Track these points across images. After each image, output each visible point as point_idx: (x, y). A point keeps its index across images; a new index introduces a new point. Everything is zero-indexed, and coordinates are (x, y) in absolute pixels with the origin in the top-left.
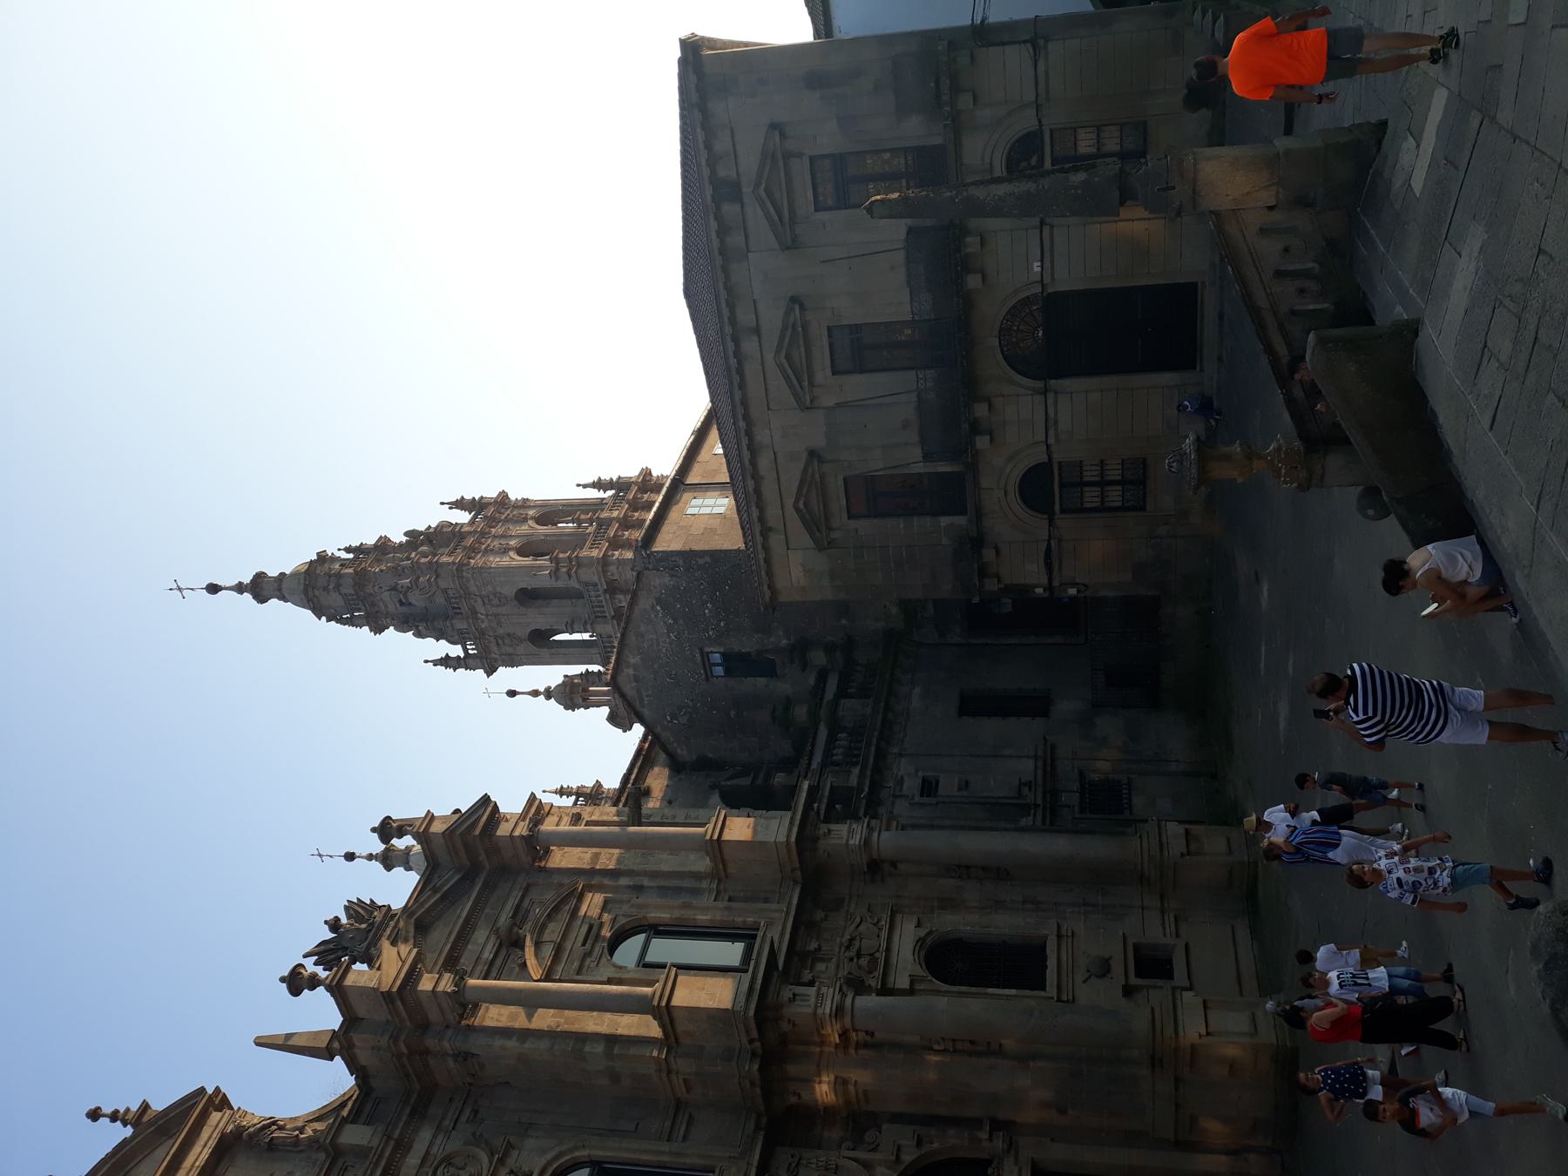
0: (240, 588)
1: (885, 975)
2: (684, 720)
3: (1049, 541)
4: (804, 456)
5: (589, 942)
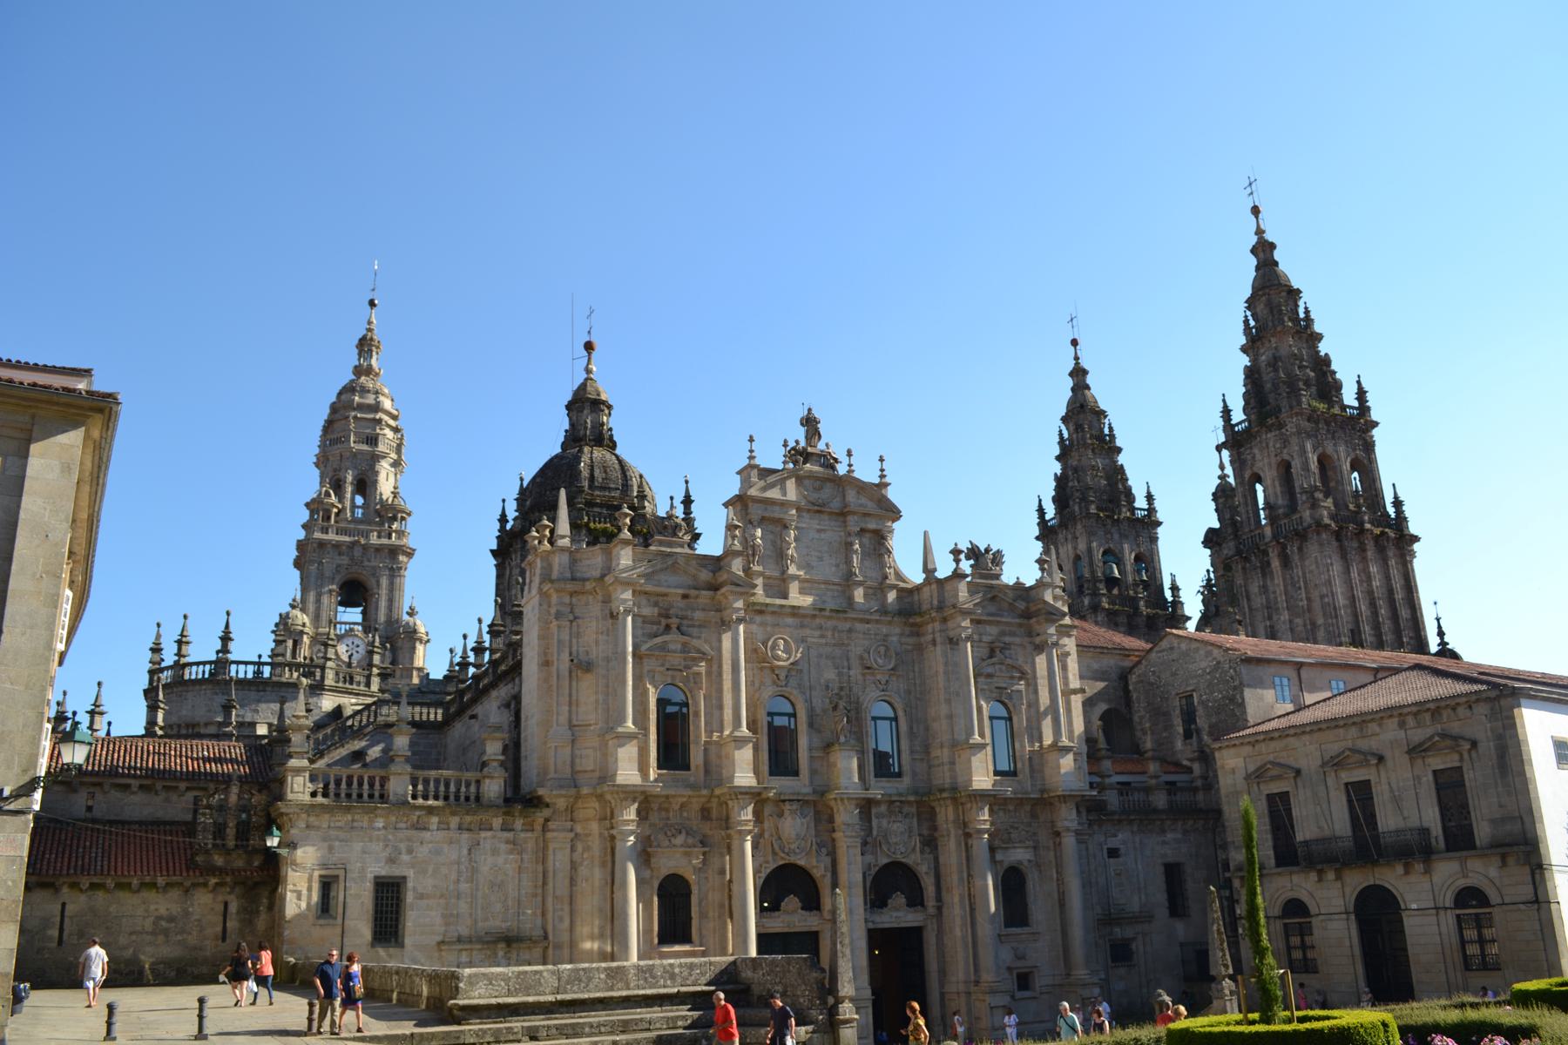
0: (1259, 232)
2: (1152, 679)
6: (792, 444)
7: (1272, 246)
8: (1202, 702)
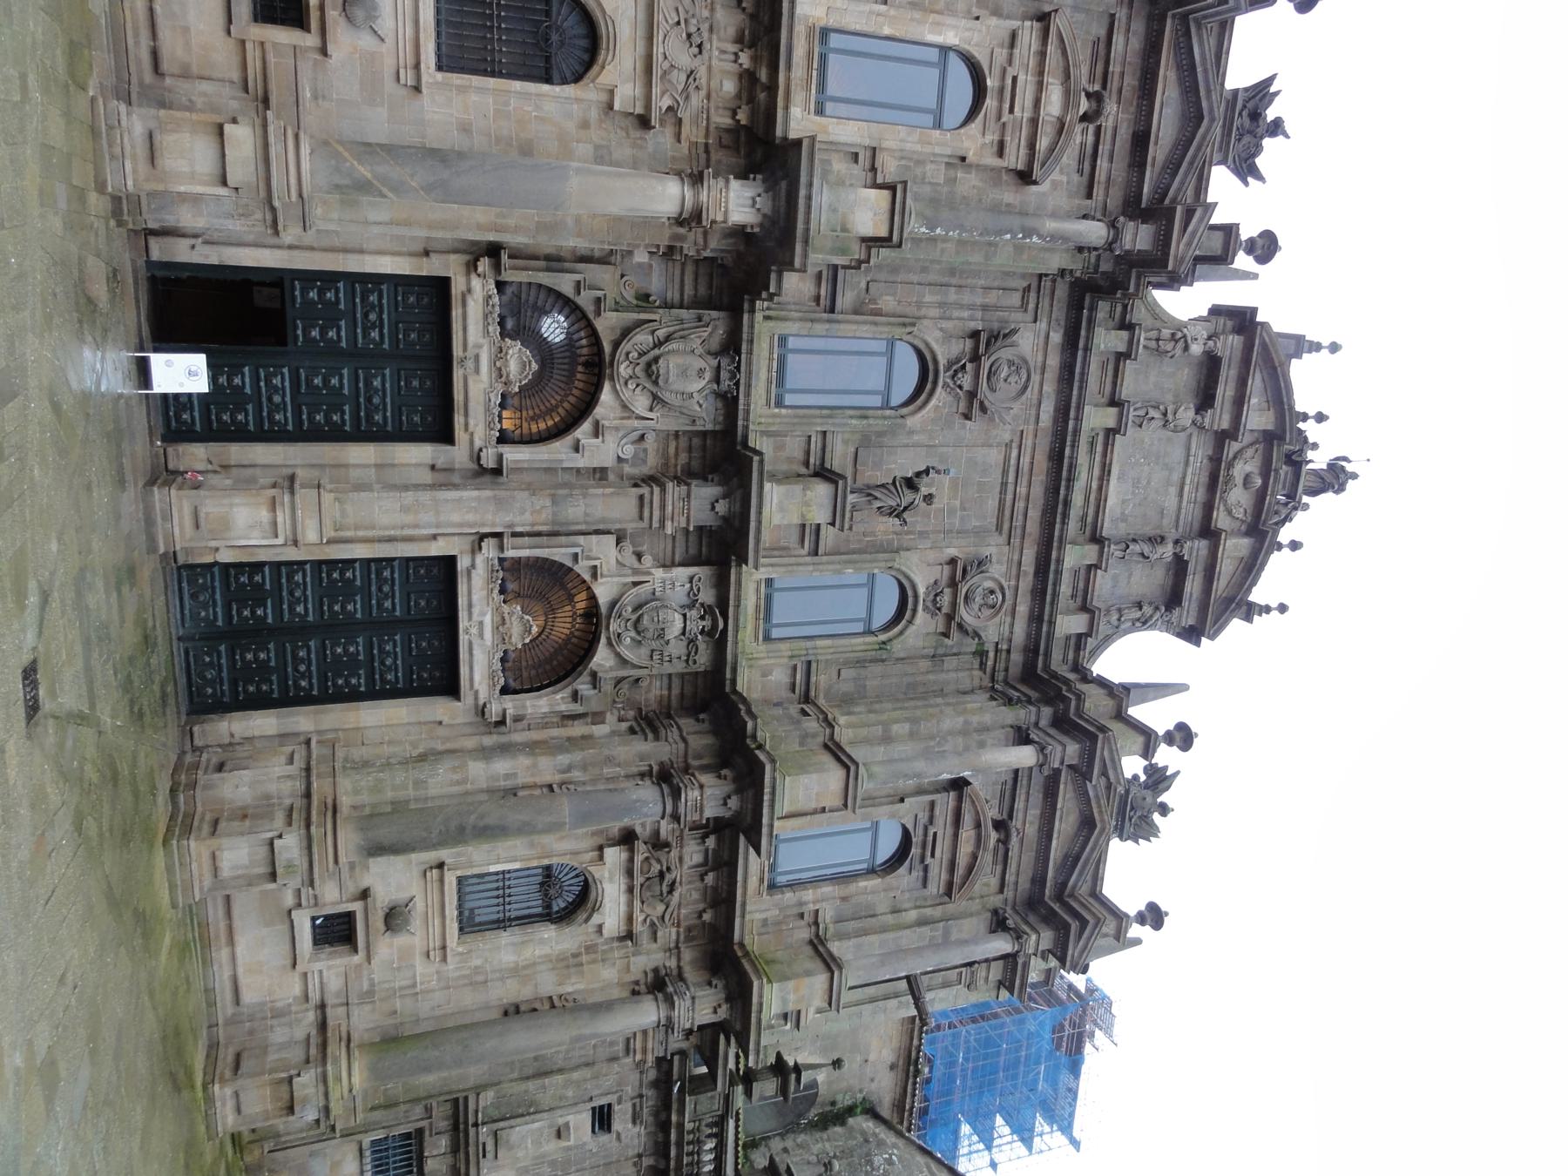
1: (631, 860)
5: (930, 838)
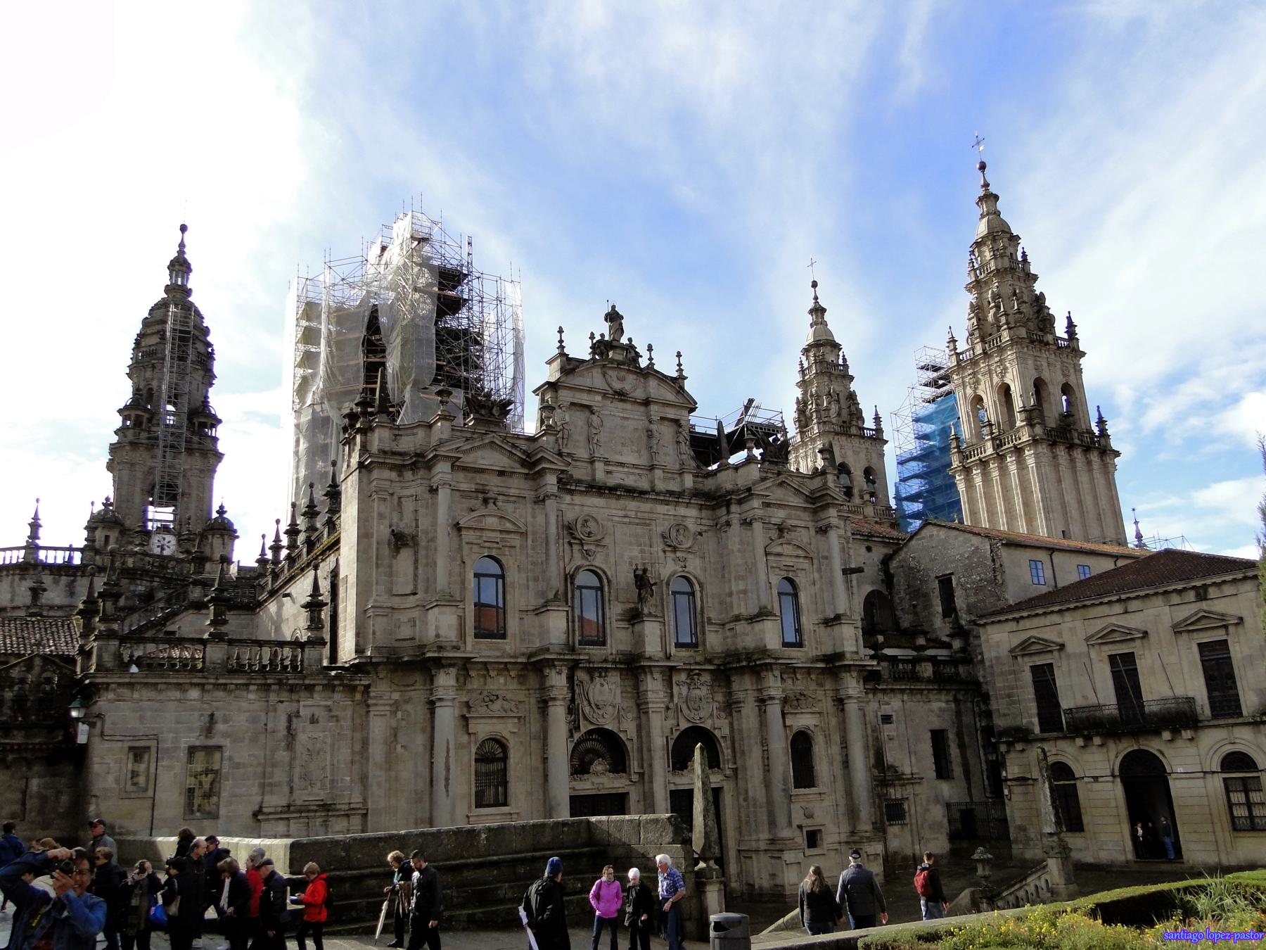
0: (986, 185)
1: (791, 713)
2: (912, 565)
3: (1032, 779)
4: (1060, 641)
5: (786, 568)
6: (598, 338)
7: (996, 197)
8: (959, 583)
